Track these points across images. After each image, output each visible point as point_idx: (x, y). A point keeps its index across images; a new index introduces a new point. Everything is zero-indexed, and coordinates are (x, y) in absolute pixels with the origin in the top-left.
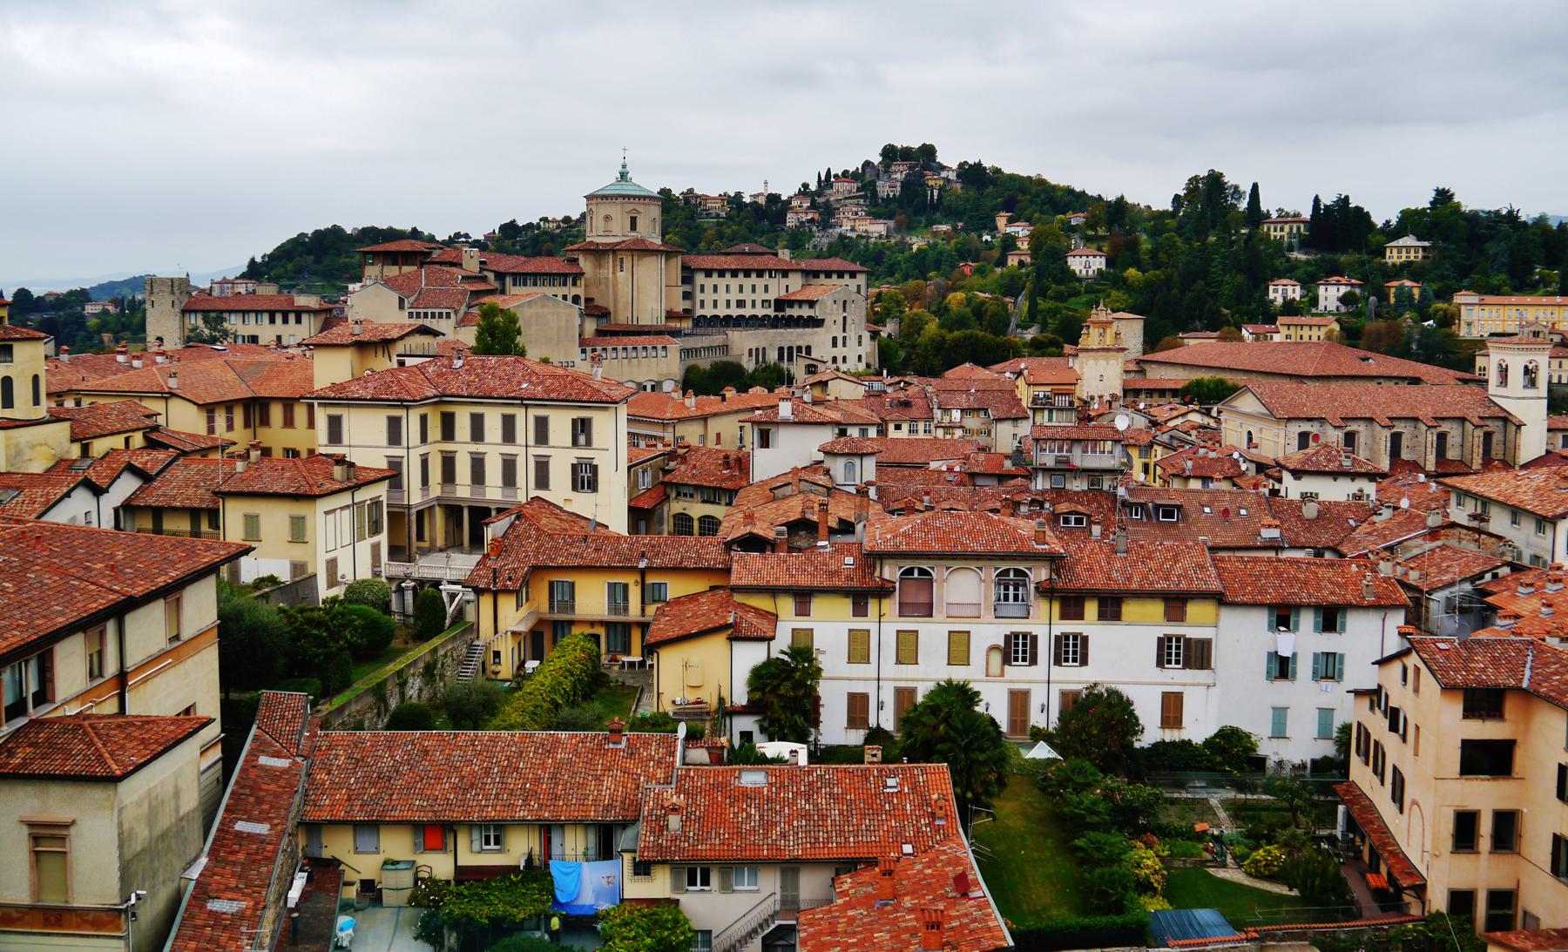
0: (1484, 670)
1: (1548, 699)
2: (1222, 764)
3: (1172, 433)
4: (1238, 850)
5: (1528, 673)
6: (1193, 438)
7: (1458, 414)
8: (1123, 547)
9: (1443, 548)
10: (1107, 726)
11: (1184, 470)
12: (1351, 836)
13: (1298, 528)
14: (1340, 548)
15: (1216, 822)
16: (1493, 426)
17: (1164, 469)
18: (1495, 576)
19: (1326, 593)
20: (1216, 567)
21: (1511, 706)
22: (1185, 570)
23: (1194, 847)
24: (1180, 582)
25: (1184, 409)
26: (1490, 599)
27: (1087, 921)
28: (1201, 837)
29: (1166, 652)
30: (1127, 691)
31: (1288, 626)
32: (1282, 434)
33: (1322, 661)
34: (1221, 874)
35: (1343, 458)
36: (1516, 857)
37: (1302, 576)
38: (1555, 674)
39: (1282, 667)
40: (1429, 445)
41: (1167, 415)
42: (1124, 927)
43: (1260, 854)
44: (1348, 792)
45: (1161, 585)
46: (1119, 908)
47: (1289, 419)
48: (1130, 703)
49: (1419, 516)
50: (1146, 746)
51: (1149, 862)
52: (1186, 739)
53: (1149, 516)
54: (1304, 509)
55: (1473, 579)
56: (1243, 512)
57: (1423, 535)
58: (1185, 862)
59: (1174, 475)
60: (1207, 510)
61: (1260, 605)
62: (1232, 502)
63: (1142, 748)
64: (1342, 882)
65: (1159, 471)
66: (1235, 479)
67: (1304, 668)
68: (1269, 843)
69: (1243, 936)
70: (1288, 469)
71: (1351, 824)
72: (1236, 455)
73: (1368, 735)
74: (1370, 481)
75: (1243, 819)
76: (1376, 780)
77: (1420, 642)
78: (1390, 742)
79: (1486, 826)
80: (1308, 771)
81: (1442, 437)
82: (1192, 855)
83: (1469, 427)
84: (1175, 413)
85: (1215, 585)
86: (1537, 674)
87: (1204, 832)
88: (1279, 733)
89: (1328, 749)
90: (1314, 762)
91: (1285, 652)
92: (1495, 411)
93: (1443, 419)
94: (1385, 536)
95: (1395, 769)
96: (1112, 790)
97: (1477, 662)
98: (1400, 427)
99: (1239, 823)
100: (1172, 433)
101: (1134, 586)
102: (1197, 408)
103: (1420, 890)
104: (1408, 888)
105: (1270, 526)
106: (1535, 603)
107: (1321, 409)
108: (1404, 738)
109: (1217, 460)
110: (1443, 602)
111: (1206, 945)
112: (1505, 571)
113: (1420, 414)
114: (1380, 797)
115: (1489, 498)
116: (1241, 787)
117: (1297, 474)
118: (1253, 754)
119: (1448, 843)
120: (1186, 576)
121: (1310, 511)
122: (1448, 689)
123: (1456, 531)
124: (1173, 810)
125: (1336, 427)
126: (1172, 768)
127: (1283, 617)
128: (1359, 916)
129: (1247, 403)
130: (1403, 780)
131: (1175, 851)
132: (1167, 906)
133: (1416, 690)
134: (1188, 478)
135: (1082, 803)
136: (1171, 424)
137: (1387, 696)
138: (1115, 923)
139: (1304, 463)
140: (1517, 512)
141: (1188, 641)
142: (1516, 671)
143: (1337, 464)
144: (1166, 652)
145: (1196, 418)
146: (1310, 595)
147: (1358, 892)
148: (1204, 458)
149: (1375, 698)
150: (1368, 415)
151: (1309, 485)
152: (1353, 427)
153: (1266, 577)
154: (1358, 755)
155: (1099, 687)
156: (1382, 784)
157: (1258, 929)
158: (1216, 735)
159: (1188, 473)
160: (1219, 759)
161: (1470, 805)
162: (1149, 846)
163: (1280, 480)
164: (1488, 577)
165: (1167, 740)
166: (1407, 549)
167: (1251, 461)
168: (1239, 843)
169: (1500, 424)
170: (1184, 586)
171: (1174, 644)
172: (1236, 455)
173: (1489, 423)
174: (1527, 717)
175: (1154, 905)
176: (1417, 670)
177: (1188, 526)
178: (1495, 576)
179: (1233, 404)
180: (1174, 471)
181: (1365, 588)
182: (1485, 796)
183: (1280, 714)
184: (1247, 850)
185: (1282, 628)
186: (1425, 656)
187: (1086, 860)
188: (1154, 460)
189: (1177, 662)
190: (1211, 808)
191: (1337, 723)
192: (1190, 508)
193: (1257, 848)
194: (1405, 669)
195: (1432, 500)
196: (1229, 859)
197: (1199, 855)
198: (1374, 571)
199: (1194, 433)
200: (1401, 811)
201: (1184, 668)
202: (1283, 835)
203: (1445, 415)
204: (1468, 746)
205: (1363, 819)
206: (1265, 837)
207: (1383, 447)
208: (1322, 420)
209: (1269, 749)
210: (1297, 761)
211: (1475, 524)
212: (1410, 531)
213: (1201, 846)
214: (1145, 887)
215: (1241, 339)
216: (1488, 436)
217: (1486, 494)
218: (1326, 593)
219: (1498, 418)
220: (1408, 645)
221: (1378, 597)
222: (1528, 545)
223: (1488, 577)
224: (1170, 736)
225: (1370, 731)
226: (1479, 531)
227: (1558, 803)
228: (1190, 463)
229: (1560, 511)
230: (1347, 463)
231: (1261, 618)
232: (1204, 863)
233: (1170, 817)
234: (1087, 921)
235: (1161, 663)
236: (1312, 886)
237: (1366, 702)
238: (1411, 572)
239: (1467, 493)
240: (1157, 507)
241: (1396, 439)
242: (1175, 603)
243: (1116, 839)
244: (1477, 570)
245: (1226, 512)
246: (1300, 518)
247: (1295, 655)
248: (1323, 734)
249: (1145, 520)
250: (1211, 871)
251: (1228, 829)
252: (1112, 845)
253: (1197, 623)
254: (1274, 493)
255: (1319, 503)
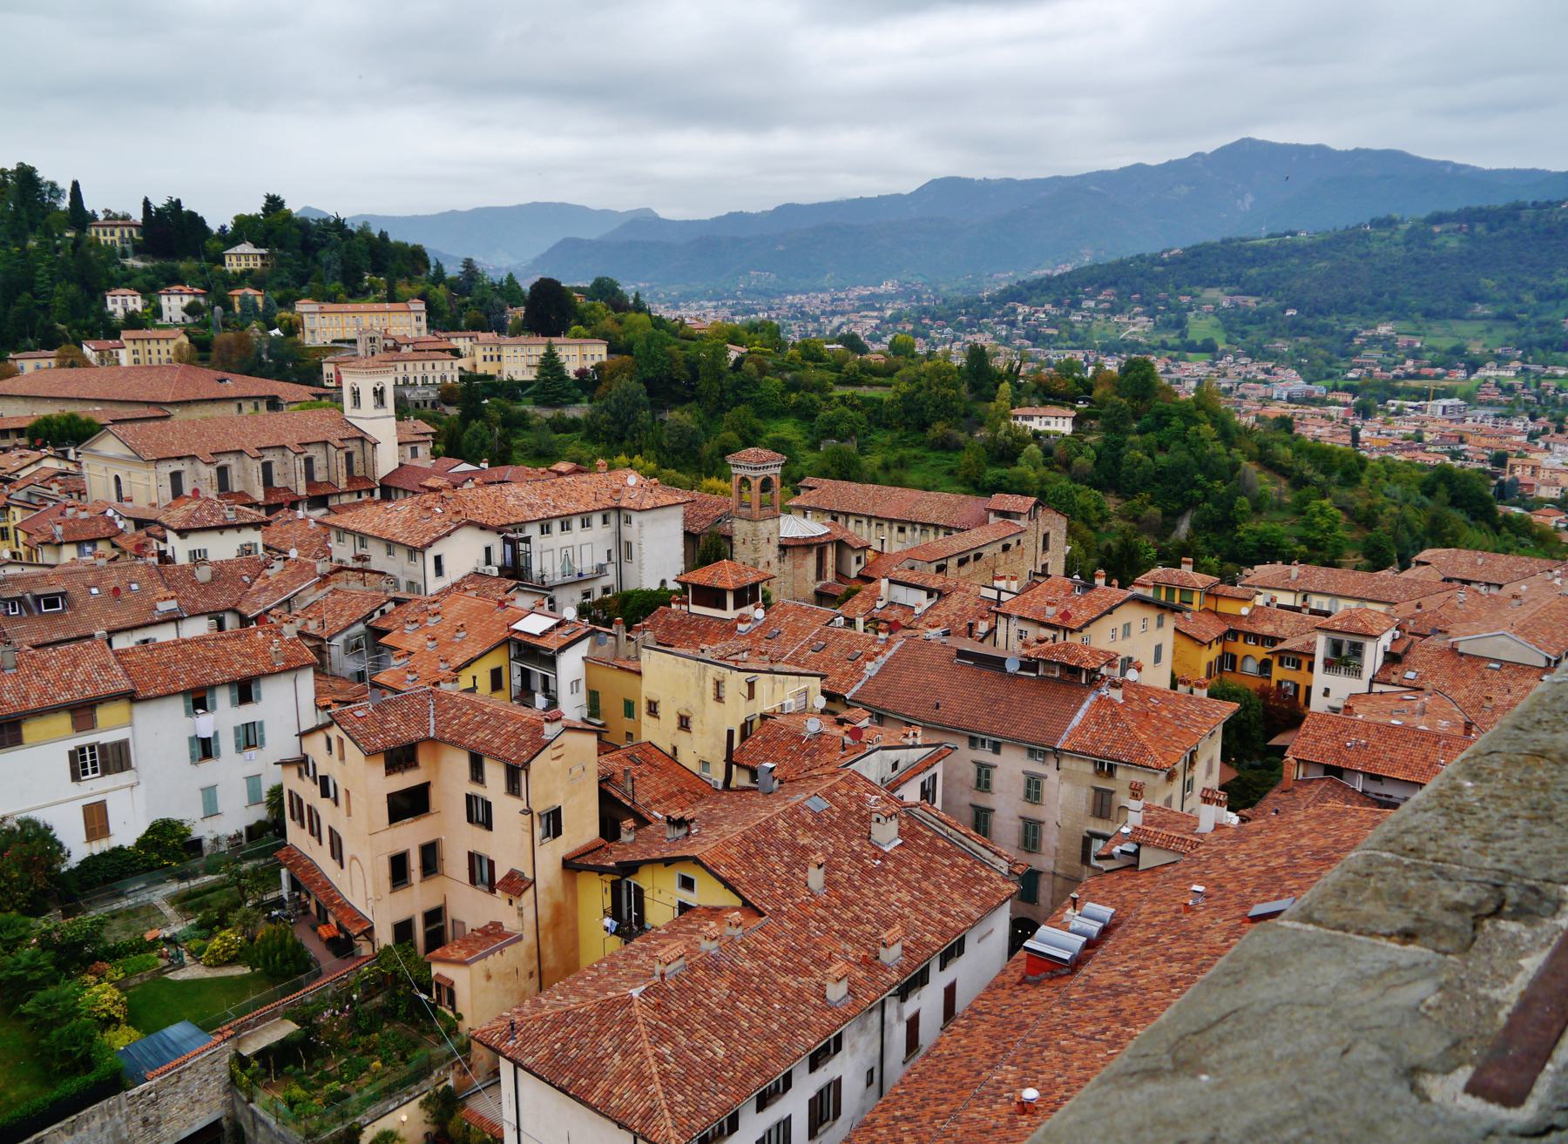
0: (397, 729)
1: (453, 743)
2: (159, 860)
3: (29, 489)
4: (193, 945)
5: (432, 722)
6: (55, 491)
7: (320, 438)
8: (10, 663)
9: (334, 592)
10: (28, 864)
11: (53, 537)
12: (297, 894)
13: (194, 593)
14: (239, 608)
15: (163, 922)
16: (353, 446)
17: (29, 534)
18: (383, 612)
19: (237, 667)
20: (120, 662)
21: (422, 756)
22: (88, 674)
23: (147, 958)
24: (84, 688)
25: (36, 455)
26: (383, 640)
27: (56, 1093)
28: (153, 945)
29: (80, 765)
30: (42, 817)
31: (205, 708)
32: (153, 477)
33: (242, 733)
34: (180, 975)
35: (226, 511)
36: (441, 878)
37: (211, 654)
38: (453, 718)
39: (205, 749)
40: (298, 471)
41: (17, 464)
42: (98, 1083)
43: (216, 943)
44: (289, 856)
45: (65, 697)
46: (87, 1064)
47: (158, 460)
48: (48, 829)
49: (308, 564)
50: (74, 866)
51: (107, 996)
52: (117, 845)
53: (29, 610)
54: (197, 573)
55: (364, 620)
56: (134, 587)
57: (316, 583)
58: (141, 977)
59: (43, 543)
60: (95, 591)
61: (175, 694)
62: (121, 578)
63: (70, 870)
64: (298, 946)
65: (22, 537)
66: (114, 539)
67: (227, 744)
68: (224, 928)
69: (219, 1038)
70: (171, 529)
71: (295, 885)
72: (110, 513)
73: (300, 801)
74: (256, 529)
75: (191, 909)
76: (314, 841)
77: (340, 714)
78: (324, 807)
79: (415, 862)
80: (244, 838)
81: (309, 462)
82: (149, 967)
83: (332, 450)
84: (26, 461)
85: (124, 685)
86: (441, 722)
87: (156, 939)
88: (211, 811)
89: (260, 813)
90: (249, 829)
91: (206, 733)
92: (352, 432)
93: (308, 444)
94: (280, 589)
95: (331, 829)
96: (48, 933)
97: (391, 722)
98: (269, 456)
99: (188, 914)
100: (29, 489)
101: (33, 705)
102: (52, 453)
103: (369, 933)
104: (359, 935)
105: (165, 599)
106: (421, 638)
107: (190, 446)
108: (337, 804)
109: (91, 519)
110: (342, 645)
111: (185, 1062)
112: (391, 606)
113: (286, 442)
114: (320, 855)
115: (366, 534)
116: (182, 877)
117: (182, 533)
118: (189, 839)
119: (387, 884)
120: (89, 681)
121: (203, 574)
122: (370, 755)
123: (343, 574)
124: (116, 924)
125: (207, 464)
126: (106, 880)
127: (199, 700)
128: (318, 975)
129: (108, 446)
130: (340, 840)
131: (129, 970)
132: (135, 1034)
133: (342, 758)
134: (61, 544)
135: (20, 962)
136: (23, 474)
137: (314, 765)
138: (88, 1083)
139: (187, 521)
140: (390, 545)
141: (103, 747)
142: (423, 723)
143: (221, 517)
144: (80, 765)
145: (52, 464)
146: (222, 672)
147: (315, 948)
148: (74, 520)
149: (303, 767)
150: (237, 448)
151: (196, 542)
152: (224, 461)
153: (176, 662)
154: (293, 819)
155: (8, 822)
156: (320, 843)
157: (232, 1024)
158: (148, 832)
159: (59, 539)
160: (156, 856)
161: (400, 849)
162: (101, 976)
163: (165, 540)
164: (377, 614)
165: (96, 852)
166: (302, 599)
167: (128, 518)
168: (192, 938)
169: (358, 443)
170: (89, 692)
171: (88, 754)
172: (110, 513)
173: (349, 443)
174: (436, 758)
175: (122, 1039)
176: (341, 741)
177: (77, 613)
178: (383, 612)
179: (93, 448)
180: (42, 539)
181: (274, 656)
182: (410, 836)
183: (209, 794)
184: (202, 942)
185: (200, 711)
186: (346, 728)
187: (42, 1025)
188: (12, 524)
189: (95, 771)
190: (155, 908)
191: (266, 787)
192: (75, 593)
193: (212, 935)
194: (329, 740)
195: (313, 536)
196: (186, 958)
197: (156, 965)
198: (279, 635)
199: (55, 487)
200: (342, 867)
201: (102, 775)
202: (234, 917)
203: (309, 440)
204: (393, 799)
205: (306, 879)
206: (218, 922)
207: (255, 478)
208: (193, 457)
209: (203, 830)
210: (232, 833)
211: (359, 565)
212: (303, 581)
213: (154, 954)
214: (110, 1022)
215: (86, 363)
216: (349, 456)
217: (363, 530)
218: (237, 667)
219: (356, 438)
220: (328, 719)
221: (288, 661)
222: (403, 573)
223: (377, 614)
224: (99, 847)
225: (301, 796)
226: (363, 571)
227: (469, 825)
228: (59, 529)
229: (427, 540)
230: (231, 516)
231: (178, 706)
232: (161, 971)
233: (116, 935)
234: (56, 1093)
235: (75, 777)
236: (274, 963)
237: (294, 771)
238: (310, 622)
239: (346, 531)
240: (37, 599)
241: (267, 468)
242: (83, 712)
243: (67, 988)
244: (367, 610)
245: (116, 590)
246: (194, 583)
247: (216, 734)
248: (254, 800)
249: (25, 614)
250: (170, 976)
251: (177, 926)
252: (65, 998)
253: (109, 728)
254: (162, 556)
255: (211, 564)
